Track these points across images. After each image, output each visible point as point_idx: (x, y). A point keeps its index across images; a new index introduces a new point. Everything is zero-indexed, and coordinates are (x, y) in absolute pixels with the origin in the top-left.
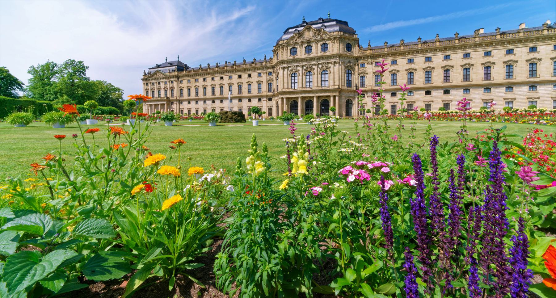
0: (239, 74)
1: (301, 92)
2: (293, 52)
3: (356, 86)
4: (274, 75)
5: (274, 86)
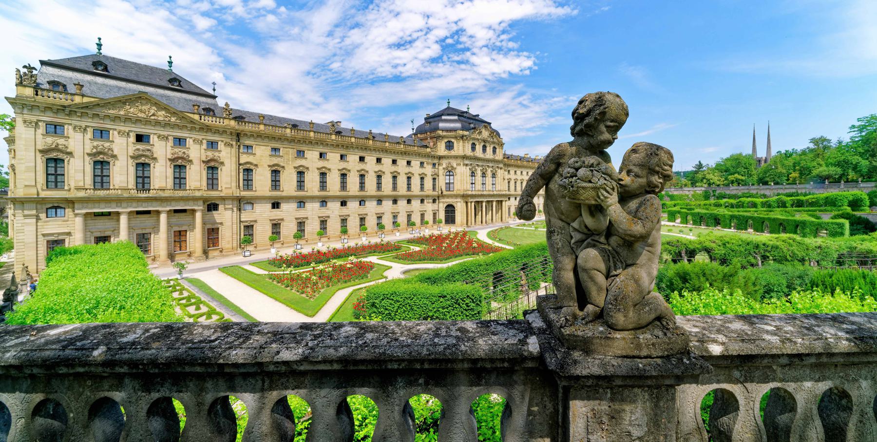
0: (394, 158)
4: (441, 168)
5: (442, 182)
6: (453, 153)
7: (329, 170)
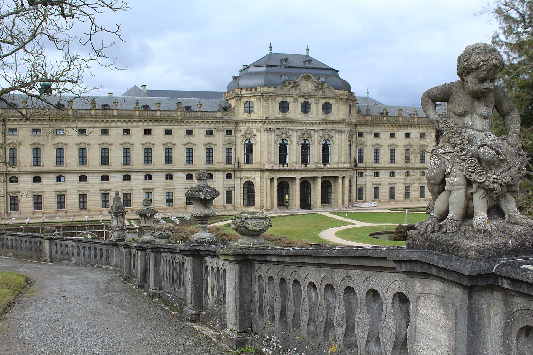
0: (168, 126)
1: (302, 171)
2: (284, 107)
3: (355, 161)
4: (238, 135)
6: (253, 116)
7: (89, 145)
